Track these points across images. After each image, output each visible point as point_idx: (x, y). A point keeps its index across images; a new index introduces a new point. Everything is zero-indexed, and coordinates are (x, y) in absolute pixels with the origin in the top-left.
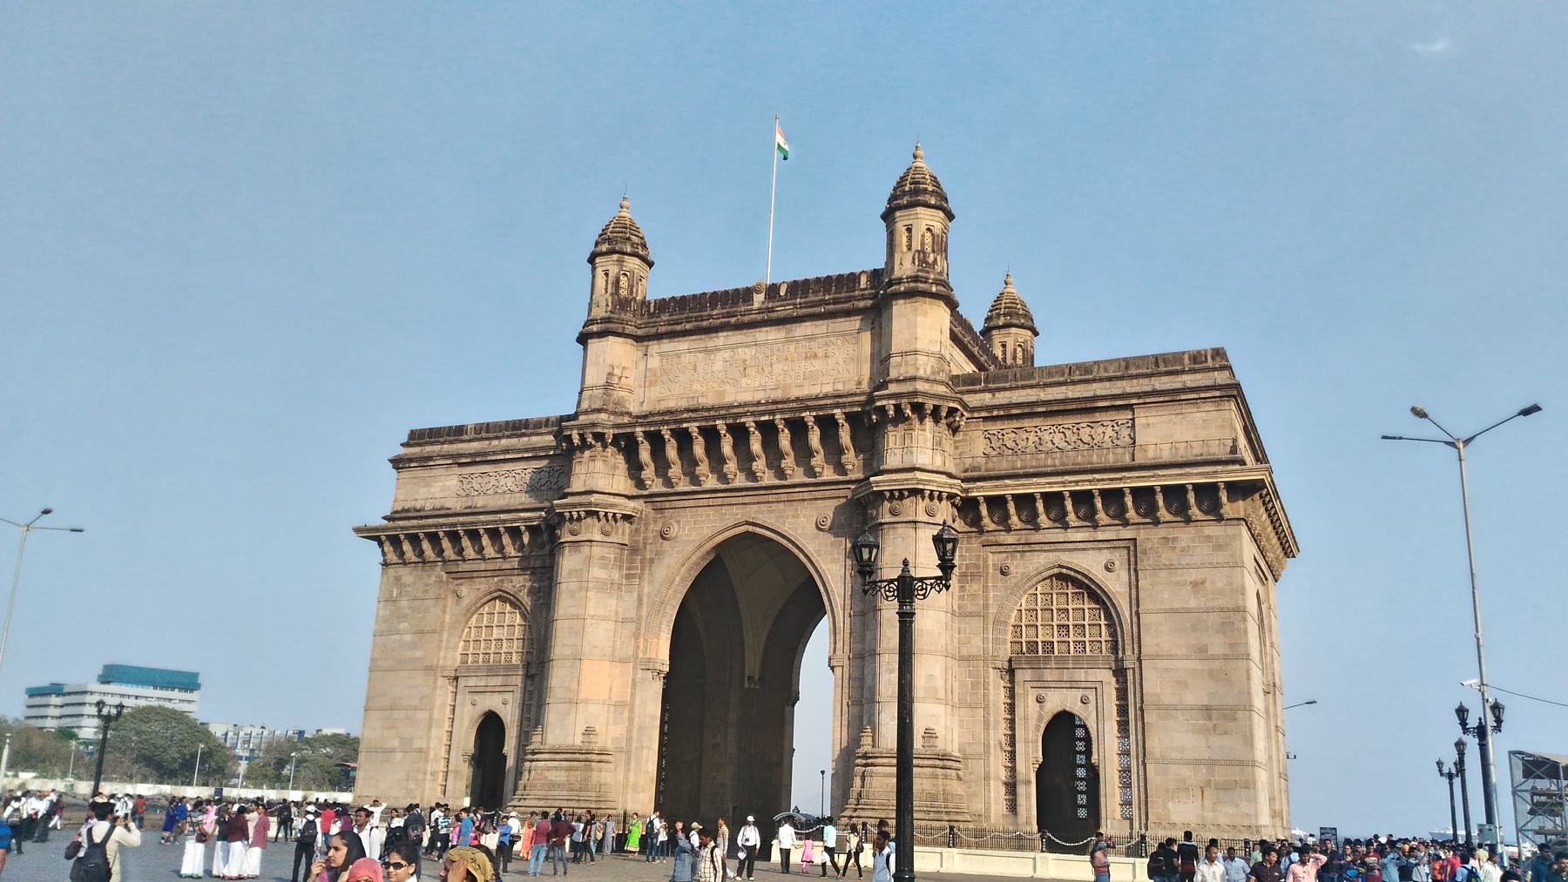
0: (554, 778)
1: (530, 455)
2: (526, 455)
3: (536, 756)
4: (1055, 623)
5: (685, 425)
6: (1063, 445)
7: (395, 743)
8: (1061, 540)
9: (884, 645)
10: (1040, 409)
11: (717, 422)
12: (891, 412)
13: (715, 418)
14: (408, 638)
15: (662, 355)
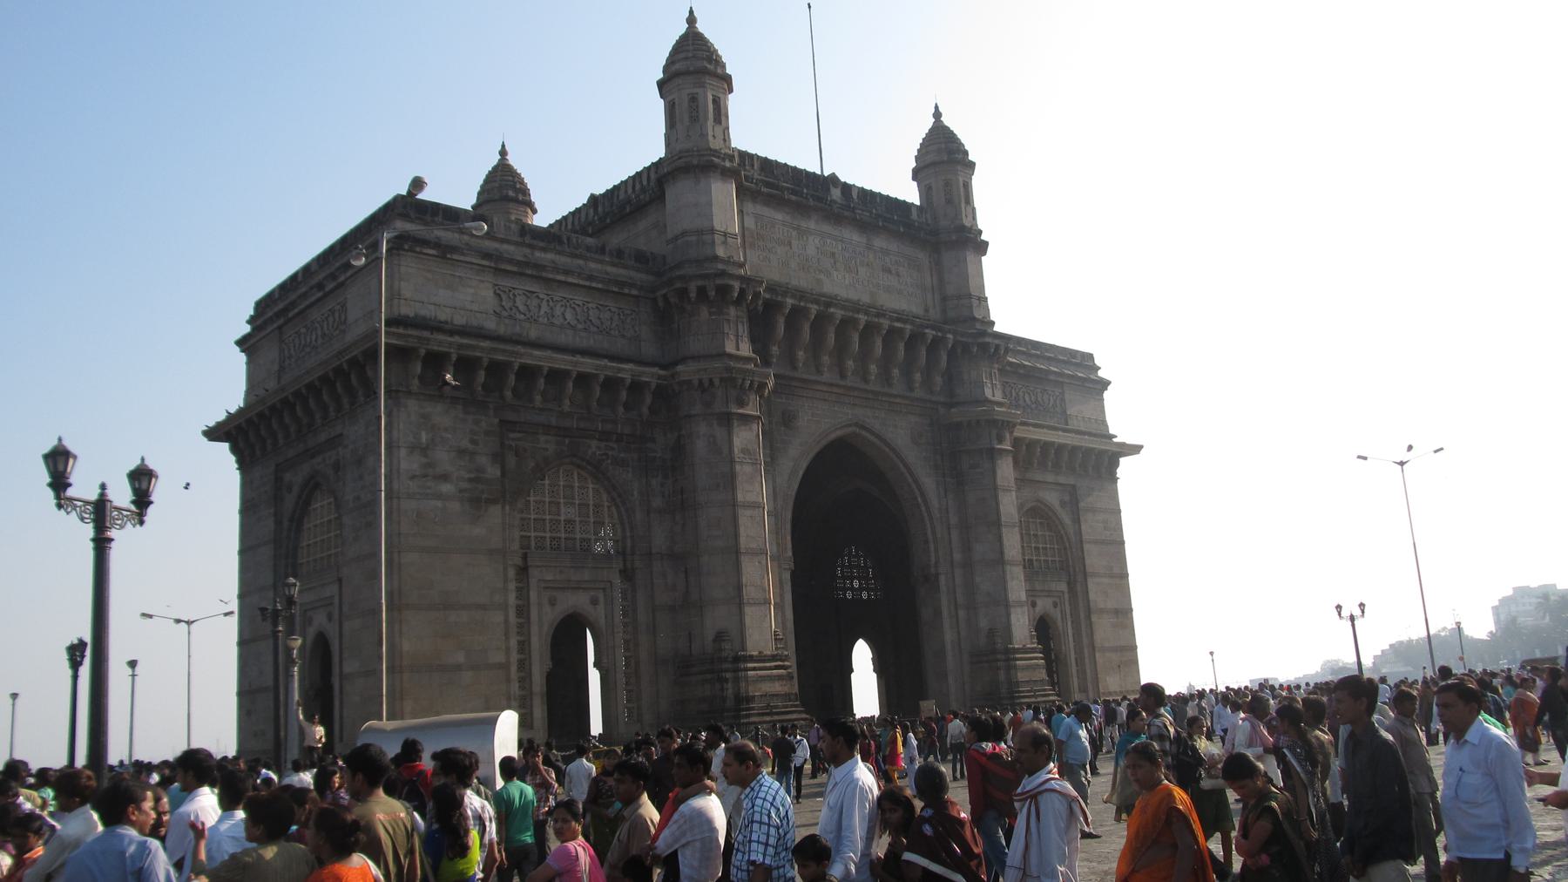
0: (768, 690)
1: (600, 286)
2: (594, 285)
3: (742, 666)
4: (1033, 545)
5: (832, 310)
6: (1029, 403)
7: (460, 658)
8: (1041, 480)
9: (1006, 557)
10: (1022, 371)
11: (860, 316)
12: (993, 350)
13: (858, 313)
14: (455, 506)
15: (757, 217)
